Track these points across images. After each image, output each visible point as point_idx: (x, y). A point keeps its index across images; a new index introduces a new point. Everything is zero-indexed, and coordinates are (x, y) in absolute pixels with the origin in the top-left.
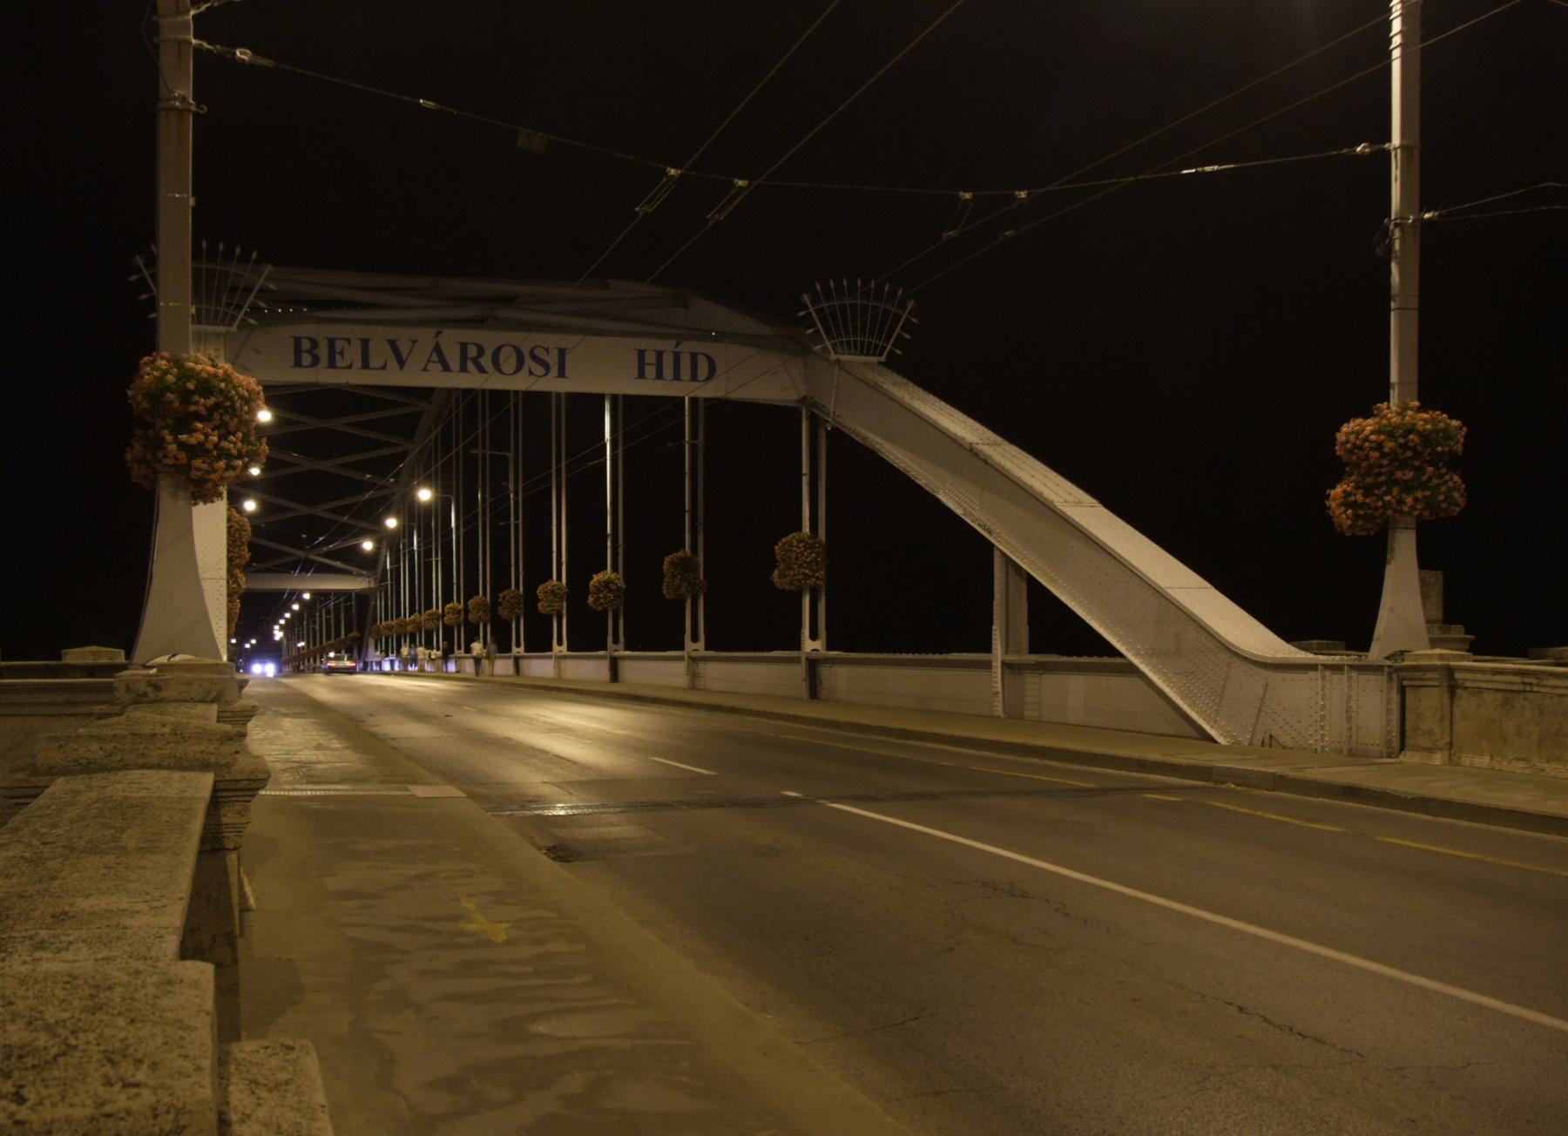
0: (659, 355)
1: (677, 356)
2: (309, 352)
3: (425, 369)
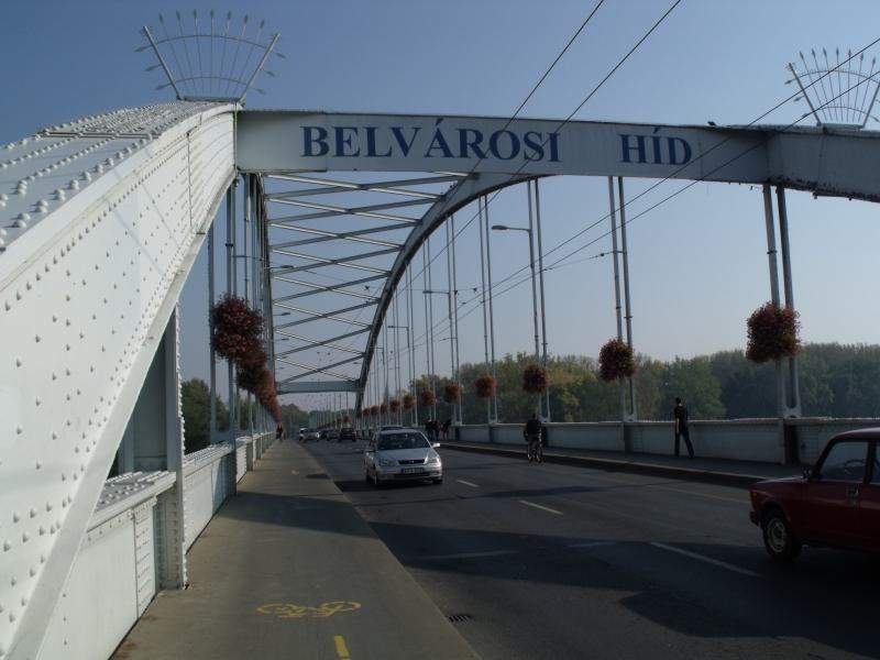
0: (641, 139)
1: (656, 141)
2: (318, 141)
3: (428, 155)
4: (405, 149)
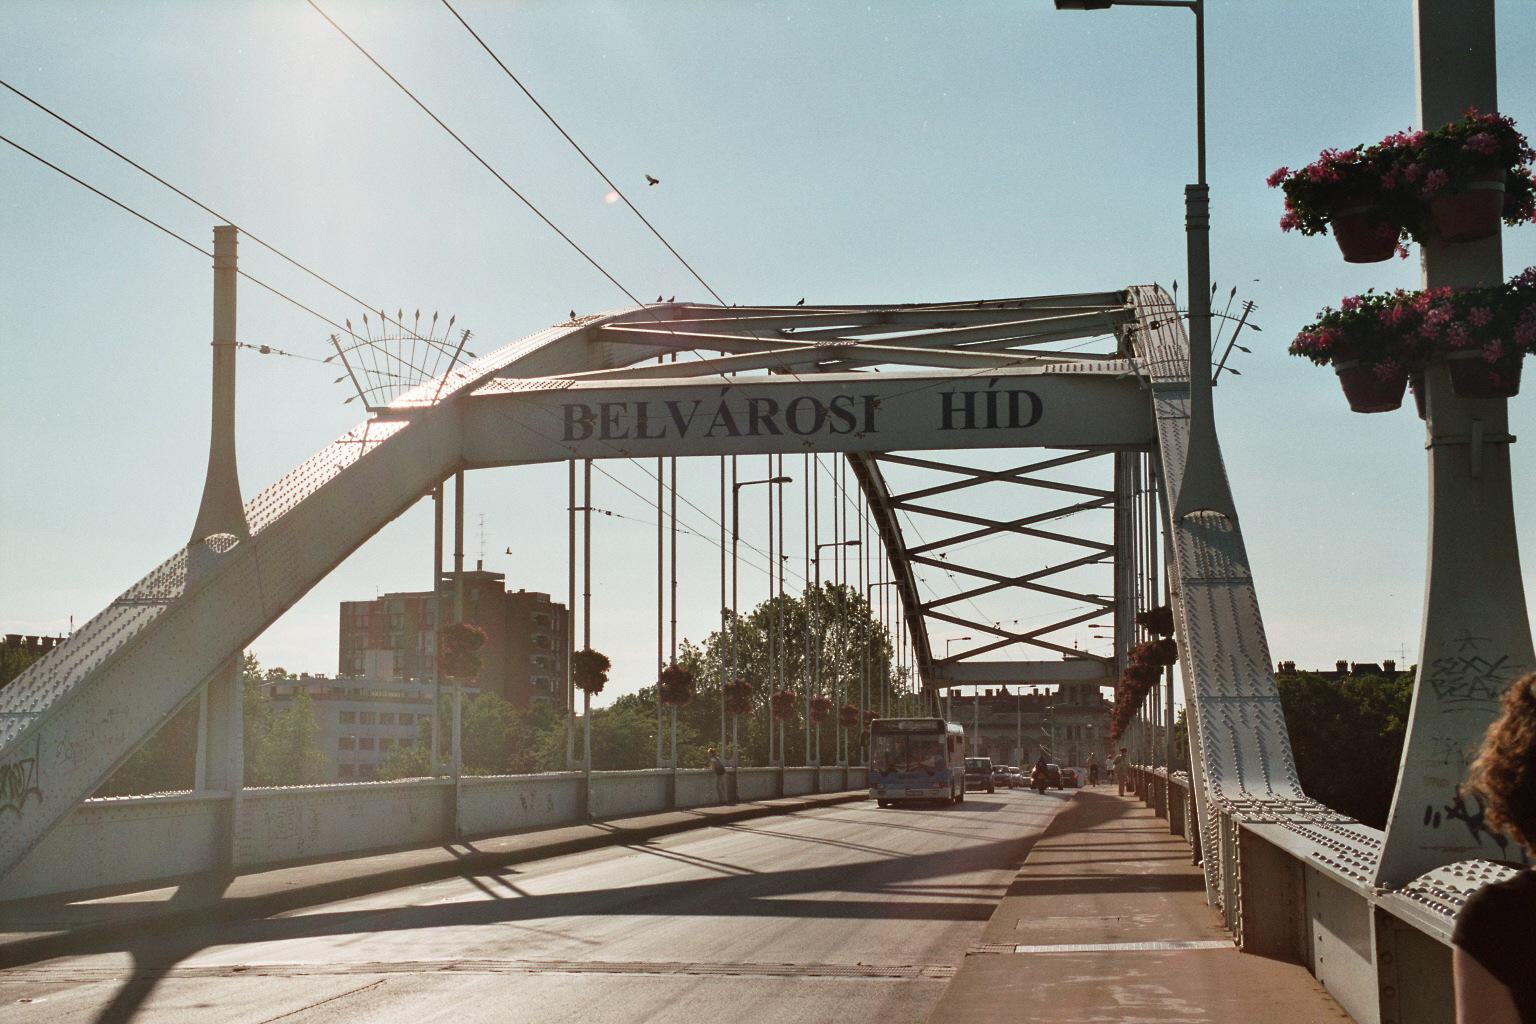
1: (992, 397)
4: (683, 429)
